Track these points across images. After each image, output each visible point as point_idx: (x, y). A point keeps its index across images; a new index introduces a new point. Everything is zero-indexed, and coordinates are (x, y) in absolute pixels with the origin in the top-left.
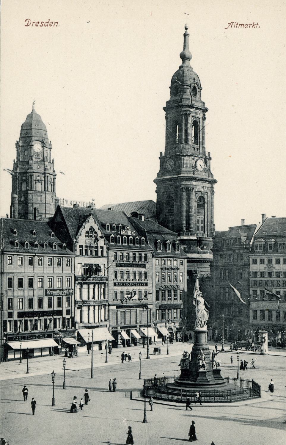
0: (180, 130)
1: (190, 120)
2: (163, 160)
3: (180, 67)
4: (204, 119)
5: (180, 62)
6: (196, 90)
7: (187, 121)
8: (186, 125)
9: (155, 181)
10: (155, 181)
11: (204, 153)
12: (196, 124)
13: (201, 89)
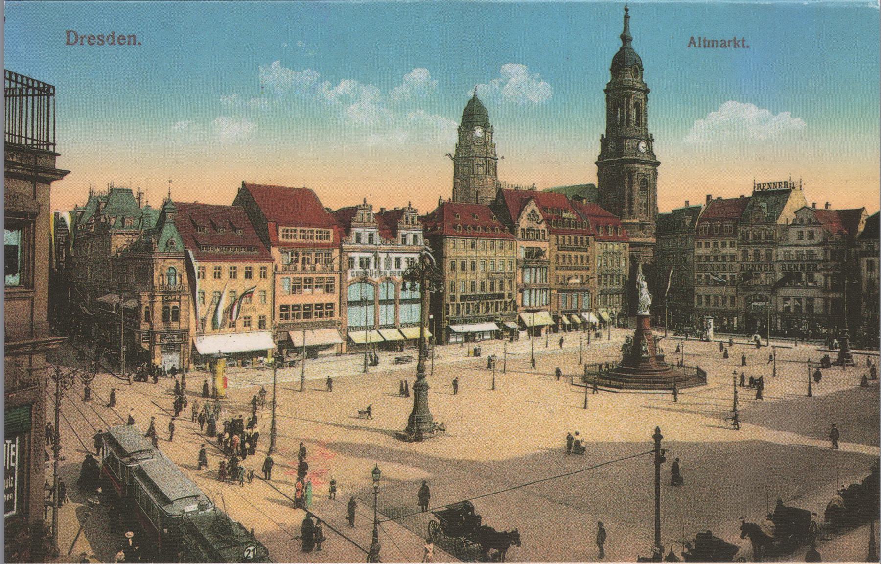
0: (622, 113)
1: (632, 103)
2: (604, 142)
3: (621, 49)
4: (646, 100)
5: (621, 44)
6: (638, 69)
7: (628, 102)
8: (628, 107)
9: (596, 163)
10: (596, 163)
11: (647, 134)
12: (637, 105)
13: (643, 70)
